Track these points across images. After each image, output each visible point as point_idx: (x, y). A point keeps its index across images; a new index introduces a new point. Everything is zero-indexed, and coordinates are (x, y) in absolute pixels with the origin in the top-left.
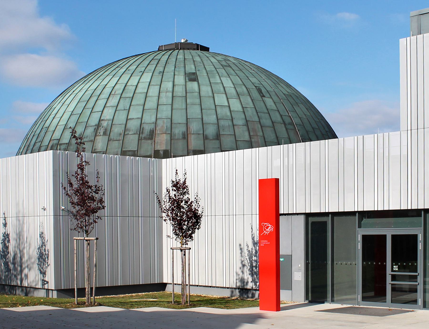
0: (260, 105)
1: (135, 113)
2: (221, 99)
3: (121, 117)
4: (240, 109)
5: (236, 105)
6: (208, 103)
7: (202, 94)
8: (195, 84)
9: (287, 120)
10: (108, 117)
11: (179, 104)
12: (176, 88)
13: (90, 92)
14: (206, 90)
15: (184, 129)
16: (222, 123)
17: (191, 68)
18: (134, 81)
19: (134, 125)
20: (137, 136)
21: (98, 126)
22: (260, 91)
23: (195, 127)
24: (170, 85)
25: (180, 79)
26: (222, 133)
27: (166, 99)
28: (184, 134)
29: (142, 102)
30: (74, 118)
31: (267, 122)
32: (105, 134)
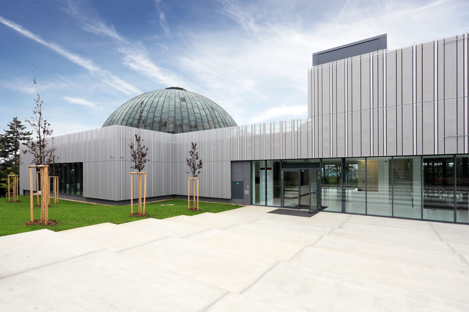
0: (213, 114)
1: (158, 114)
2: (196, 110)
3: (151, 115)
4: (205, 115)
5: (203, 113)
6: (191, 111)
7: (188, 107)
8: (185, 103)
9: (224, 121)
10: (144, 115)
11: (178, 110)
12: (176, 104)
13: (135, 104)
14: (189, 106)
15: (181, 122)
16: (197, 120)
17: (182, 96)
18: (156, 100)
19: (157, 119)
20: (159, 125)
21: (139, 120)
22: (212, 108)
23: (186, 121)
24: (174, 102)
25: (178, 100)
26: (198, 125)
27: (172, 108)
28: (181, 124)
29: (161, 109)
30: (128, 115)
31: (216, 121)
32: (143, 123)
